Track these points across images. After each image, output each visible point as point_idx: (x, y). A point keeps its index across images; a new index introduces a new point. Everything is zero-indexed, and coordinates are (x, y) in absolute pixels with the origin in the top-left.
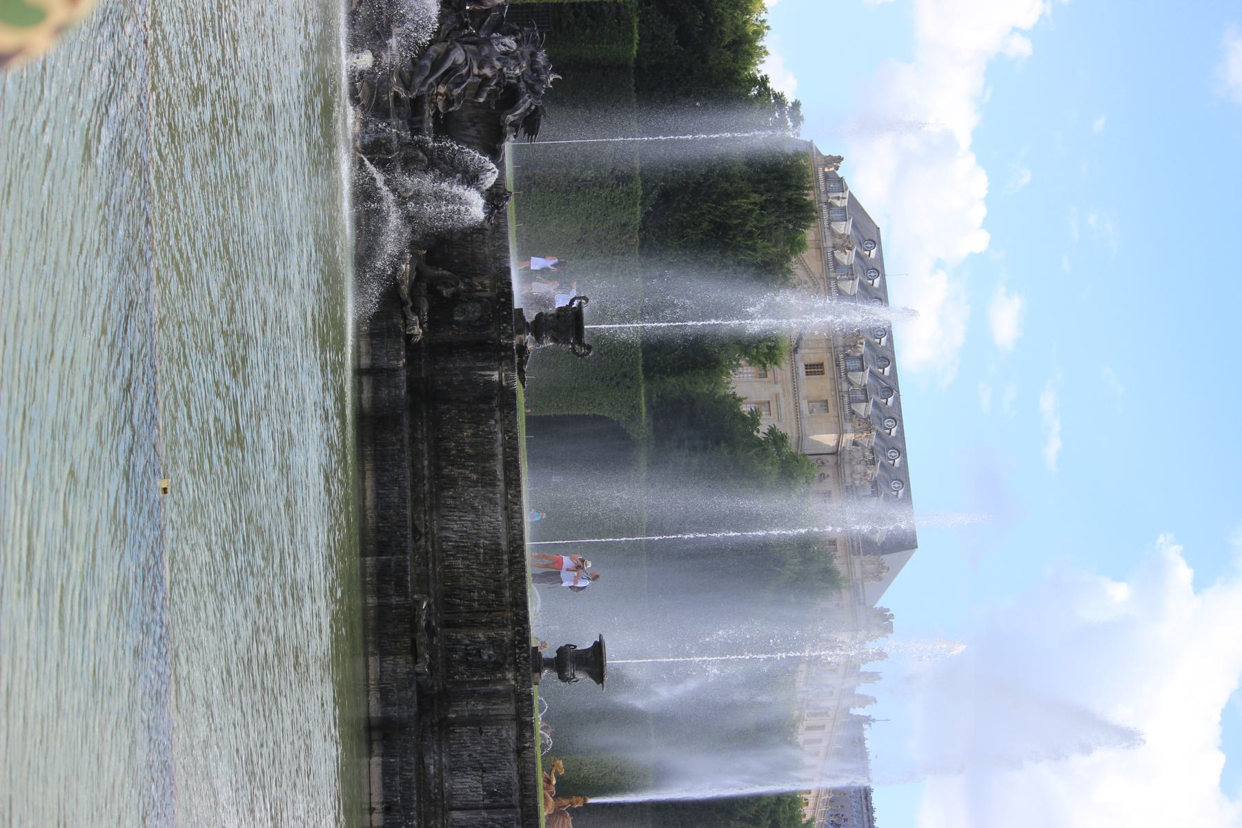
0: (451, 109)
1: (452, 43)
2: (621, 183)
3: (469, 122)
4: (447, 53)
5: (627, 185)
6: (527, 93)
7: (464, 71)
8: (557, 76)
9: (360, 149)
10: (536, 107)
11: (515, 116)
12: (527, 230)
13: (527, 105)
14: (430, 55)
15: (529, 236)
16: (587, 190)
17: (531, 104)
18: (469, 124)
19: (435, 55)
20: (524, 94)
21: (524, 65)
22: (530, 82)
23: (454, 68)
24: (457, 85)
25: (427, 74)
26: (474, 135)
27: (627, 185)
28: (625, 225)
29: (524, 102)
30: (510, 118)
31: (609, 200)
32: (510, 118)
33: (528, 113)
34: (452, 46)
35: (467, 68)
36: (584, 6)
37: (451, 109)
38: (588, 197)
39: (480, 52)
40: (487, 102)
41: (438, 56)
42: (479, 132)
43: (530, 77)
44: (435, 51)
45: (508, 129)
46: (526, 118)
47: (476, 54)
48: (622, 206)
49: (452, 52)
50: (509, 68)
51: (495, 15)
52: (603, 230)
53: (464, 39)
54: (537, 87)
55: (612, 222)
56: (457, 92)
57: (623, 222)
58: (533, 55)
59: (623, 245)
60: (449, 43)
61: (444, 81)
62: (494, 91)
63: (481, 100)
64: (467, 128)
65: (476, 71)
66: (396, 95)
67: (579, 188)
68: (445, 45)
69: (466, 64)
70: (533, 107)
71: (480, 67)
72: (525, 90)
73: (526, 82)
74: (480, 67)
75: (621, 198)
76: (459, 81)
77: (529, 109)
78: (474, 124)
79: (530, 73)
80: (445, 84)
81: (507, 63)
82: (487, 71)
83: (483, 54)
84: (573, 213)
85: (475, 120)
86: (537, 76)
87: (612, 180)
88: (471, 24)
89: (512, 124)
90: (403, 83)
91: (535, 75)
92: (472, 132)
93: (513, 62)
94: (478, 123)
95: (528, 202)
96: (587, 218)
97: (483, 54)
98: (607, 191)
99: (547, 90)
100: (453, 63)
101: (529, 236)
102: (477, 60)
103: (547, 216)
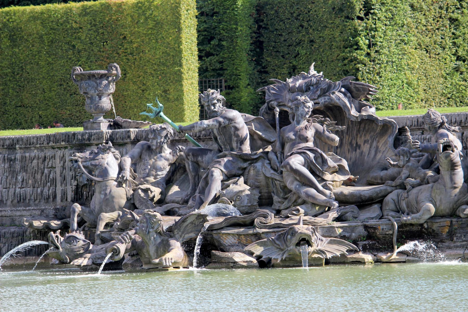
0: (347, 168)
1: (285, 166)
2: (372, 11)
3: (356, 151)
4: (296, 172)
5: (373, 5)
6: (330, 96)
7: (312, 155)
8: (312, 67)
9: (389, 254)
10: (343, 86)
11: (351, 107)
12: (416, 101)
13: (341, 96)
14: (296, 187)
15: (422, 100)
16: (378, 43)
17: (340, 91)
18: (358, 150)
19: (296, 183)
20: (331, 99)
21: (303, 98)
22: (319, 93)
23: (309, 165)
24: (324, 161)
25: (313, 191)
26: (368, 146)
27: (373, 5)
28: (412, 6)
29: (339, 99)
30: (354, 112)
31: (388, 23)
32: (354, 112)
33: (349, 94)
34: (288, 167)
35: (308, 152)
36: (200, 47)
37: (347, 168)
38: (385, 44)
39: (291, 140)
40: (337, 133)
41: (296, 180)
42: (365, 142)
43: (314, 93)
44: (292, 183)
45: (364, 113)
46: (353, 97)
47: (294, 144)
48: (394, 9)
49: (294, 167)
50: (307, 113)
51: (255, 127)
52: (417, 28)
53: (279, 155)
54: (324, 86)
55: (409, 20)
56: (331, 163)
57: (409, 8)
58: (292, 90)
59: (432, 7)
60: (284, 170)
61: (320, 175)
62: (327, 125)
63: (337, 139)
64: (362, 153)
65: (310, 144)
66: (337, 219)
67: (376, 51)
68: (285, 174)
69: (304, 153)
70: (343, 90)
71: (306, 140)
72: (327, 98)
73: (319, 96)
74: (306, 140)
75: (386, 11)
76: (320, 160)
77: (345, 94)
78: (358, 146)
79: (310, 93)
80: (323, 174)
81: (302, 115)
82: (310, 134)
83: (293, 137)
84: (400, 57)
85: (355, 145)
86: (313, 86)
87: (368, 19)
88: (264, 149)
89: (359, 111)
90: (322, 213)
91: (311, 88)
92: (365, 148)
93: (301, 109)
94: (357, 143)
95: (389, 101)
96: (405, 44)
97: (293, 137)
98: (379, 24)
99: (325, 76)
100: (304, 166)
101: (422, 100)
102: (299, 143)
103: (403, 82)
